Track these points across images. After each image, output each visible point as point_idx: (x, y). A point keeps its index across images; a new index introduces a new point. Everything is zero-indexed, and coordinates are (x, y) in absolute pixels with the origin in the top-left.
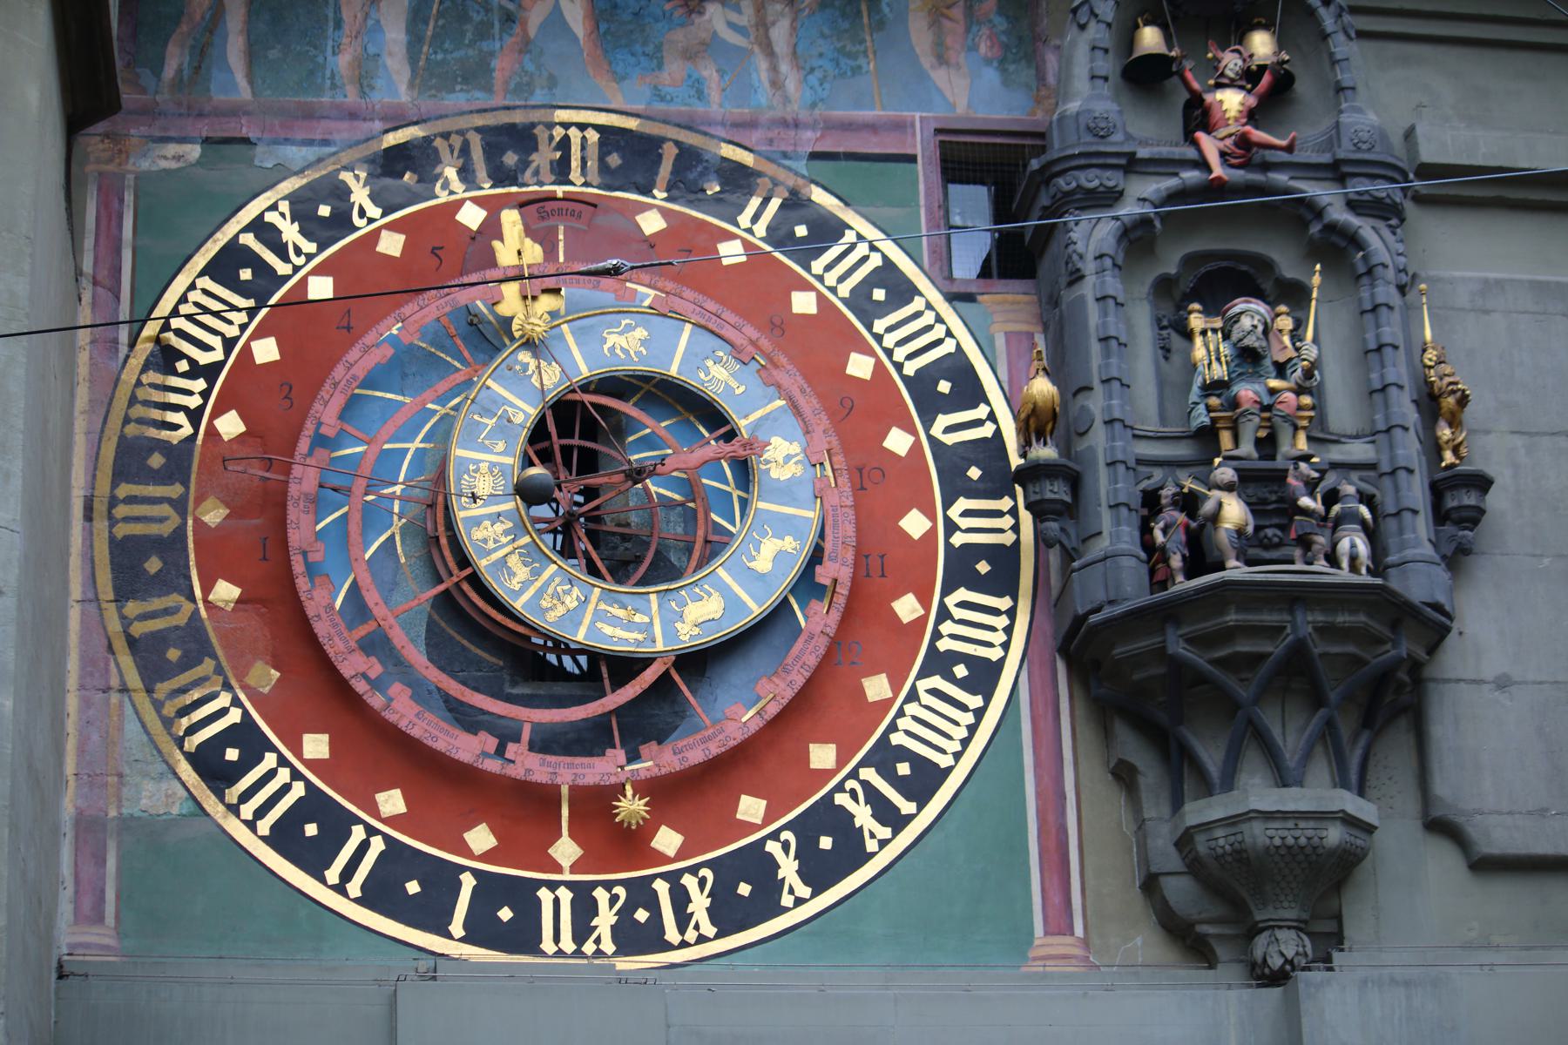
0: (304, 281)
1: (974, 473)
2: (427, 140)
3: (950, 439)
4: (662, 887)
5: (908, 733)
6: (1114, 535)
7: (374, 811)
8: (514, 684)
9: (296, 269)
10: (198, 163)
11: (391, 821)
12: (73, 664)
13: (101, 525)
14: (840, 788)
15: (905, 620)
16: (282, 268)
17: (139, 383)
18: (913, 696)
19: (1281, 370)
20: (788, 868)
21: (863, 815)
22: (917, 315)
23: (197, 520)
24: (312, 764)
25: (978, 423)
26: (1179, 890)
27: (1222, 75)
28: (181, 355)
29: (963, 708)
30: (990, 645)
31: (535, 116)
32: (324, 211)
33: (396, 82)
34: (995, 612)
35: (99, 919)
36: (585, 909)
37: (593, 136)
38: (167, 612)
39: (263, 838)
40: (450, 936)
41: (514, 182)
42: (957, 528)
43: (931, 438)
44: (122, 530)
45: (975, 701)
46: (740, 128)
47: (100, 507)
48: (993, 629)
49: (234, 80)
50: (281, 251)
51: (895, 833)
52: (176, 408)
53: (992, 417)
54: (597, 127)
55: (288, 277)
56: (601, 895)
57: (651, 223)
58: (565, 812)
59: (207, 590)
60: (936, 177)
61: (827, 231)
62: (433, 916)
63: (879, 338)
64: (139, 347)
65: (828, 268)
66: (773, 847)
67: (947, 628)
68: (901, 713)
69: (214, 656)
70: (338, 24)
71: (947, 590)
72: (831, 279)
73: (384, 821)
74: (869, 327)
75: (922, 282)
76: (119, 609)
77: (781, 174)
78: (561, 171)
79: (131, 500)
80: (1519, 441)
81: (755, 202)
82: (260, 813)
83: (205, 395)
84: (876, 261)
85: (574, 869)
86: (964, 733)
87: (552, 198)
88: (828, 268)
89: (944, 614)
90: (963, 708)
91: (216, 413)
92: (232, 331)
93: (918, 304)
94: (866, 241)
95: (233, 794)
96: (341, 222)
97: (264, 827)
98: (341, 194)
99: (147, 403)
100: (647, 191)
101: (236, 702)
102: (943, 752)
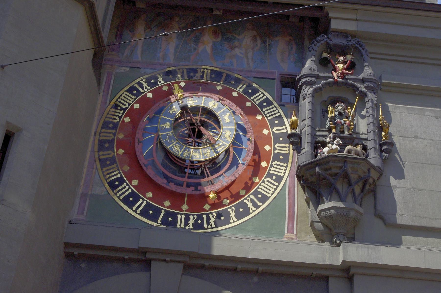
0: (146, 94)
1: (281, 139)
2: (175, 70)
3: (276, 132)
4: (205, 216)
5: (261, 189)
6: (307, 147)
7: (145, 196)
8: (179, 173)
9: (145, 91)
10: (129, 71)
11: (148, 199)
12: (86, 163)
13: (97, 137)
14: (246, 199)
15: (263, 166)
16: (142, 91)
17: (110, 111)
18: (263, 182)
19: (347, 118)
20: (232, 215)
21: (250, 205)
22: (272, 108)
23: (117, 137)
24: (133, 186)
25: (283, 129)
26: (319, 226)
27: (339, 61)
28: (119, 106)
29: (274, 185)
30: (281, 173)
31: (198, 67)
32: (153, 81)
33: (171, 59)
34: (283, 166)
35: (82, 213)
36: (187, 219)
37: (209, 71)
38: (108, 154)
39: (121, 200)
40: (157, 223)
41: (192, 78)
42: (276, 149)
43: (272, 132)
44: (101, 138)
45: (277, 184)
46: (239, 72)
47: (98, 133)
48: (282, 170)
49: (138, 56)
50: (143, 88)
51: (256, 210)
52: (116, 116)
53: (286, 128)
54: (210, 70)
55: (143, 93)
56: (191, 217)
57: (219, 88)
58: (186, 199)
59: (117, 150)
60: (279, 83)
61: (255, 91)
62: (154, 218)
63: (264, 112)
64: (111, 103)
65: (255, 98)
66: (230, 210)
67: (272, 169)
68: (260, 185)
69: (117, 164)
70: (160, 48)
71: (273, 161)
72: (255, 100)
73: (147, 199)
74: (262, 110)
75: (274, 102)
76: (98, 153)
77: (247, 81)
78: (202, 77)
79: (104, 132)
80: (401, 138)
81: (241, 85)
82: (121, 195)
83: (123, 114)
84: (265, 97)
85: (186, 211)
86: (273, 190)
87: (199, 82)
88: (255, 98)
89: (272, 166)
90: (274, 185)
91: (125, 117)
92: (130, 102)
93: (273, 106)
94: (263, 94)
95: (115, 191)
96: (156, 83)
97: (121, 198)
98: (156, 79)
99: (111, 114)
100: (219, 82)
101: (120, 173)
102: (269, 193)
